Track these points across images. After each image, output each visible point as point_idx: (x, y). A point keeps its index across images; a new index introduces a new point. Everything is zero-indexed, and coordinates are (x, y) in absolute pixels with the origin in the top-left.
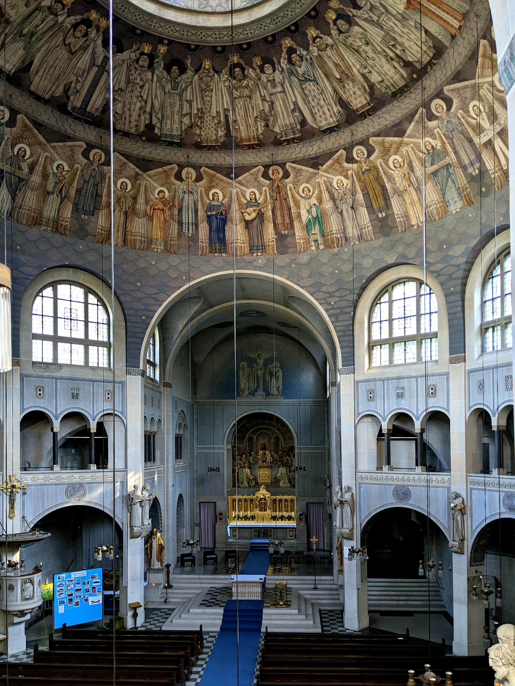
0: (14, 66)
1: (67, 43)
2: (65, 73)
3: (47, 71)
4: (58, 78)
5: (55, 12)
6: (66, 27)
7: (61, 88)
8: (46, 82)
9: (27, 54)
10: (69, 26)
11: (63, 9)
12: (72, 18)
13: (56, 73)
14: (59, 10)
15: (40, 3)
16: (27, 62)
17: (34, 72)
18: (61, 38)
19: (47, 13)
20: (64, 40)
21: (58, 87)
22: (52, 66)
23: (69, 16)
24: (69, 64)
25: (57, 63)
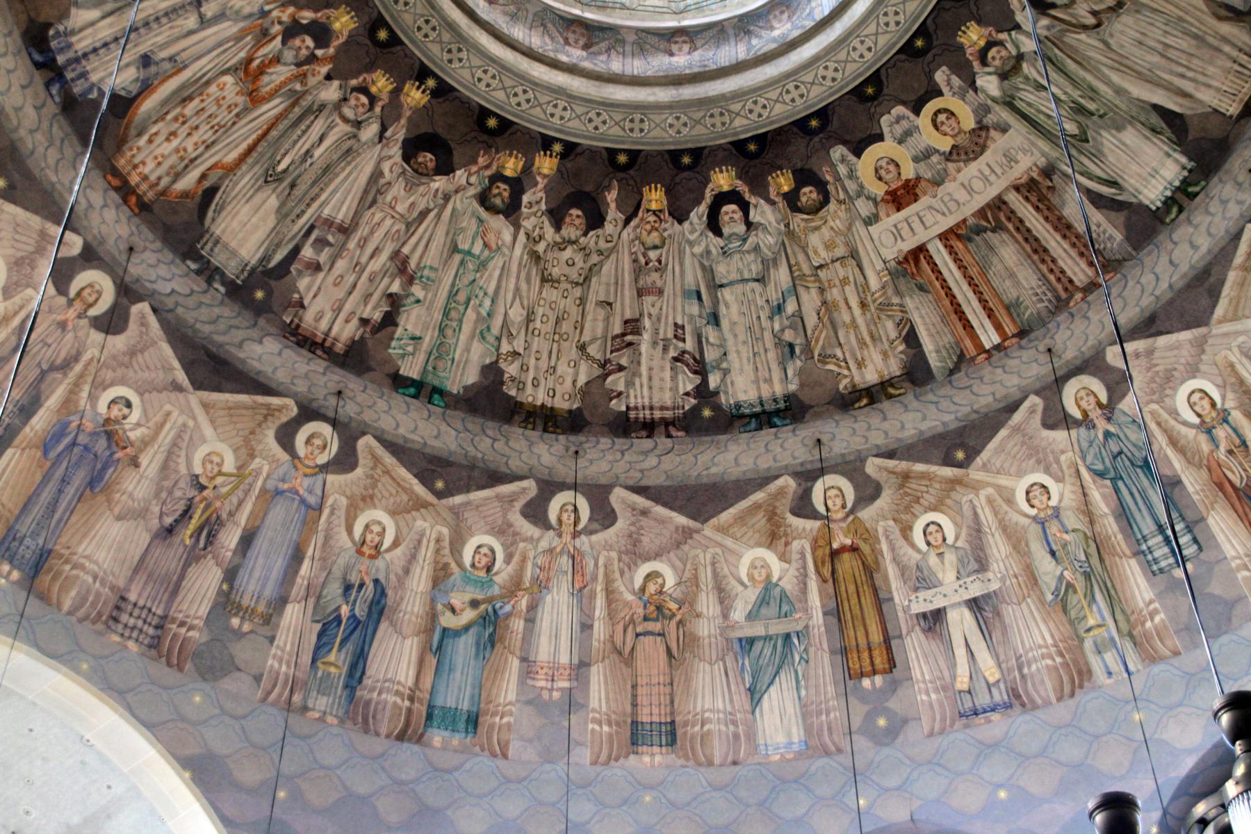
0: (1169, 155)
1: (1091, 21)
2: (1180, 19)
3: (1181, 70)
4: (1196, 37)
5: (1012, 62)
6: (1048, 28)
7: (1226, 28)
8: (1211, 70)
9: (1133, 120)
10: (1045, 22)
11: (1001, 43)
12: (1019, 18)
13: (1185, 43)
14: (1004, 53)
15: (994, 100)
16: (1155, 120)
17: (1180, 100)
18: (1083, 37)
19: (1018, 81)
20: (1085, 28)
21: (1224, 39)
22: (1163, 56)
23: (1017, 27)
24: (1155, 10)
25: (1152, 44)
